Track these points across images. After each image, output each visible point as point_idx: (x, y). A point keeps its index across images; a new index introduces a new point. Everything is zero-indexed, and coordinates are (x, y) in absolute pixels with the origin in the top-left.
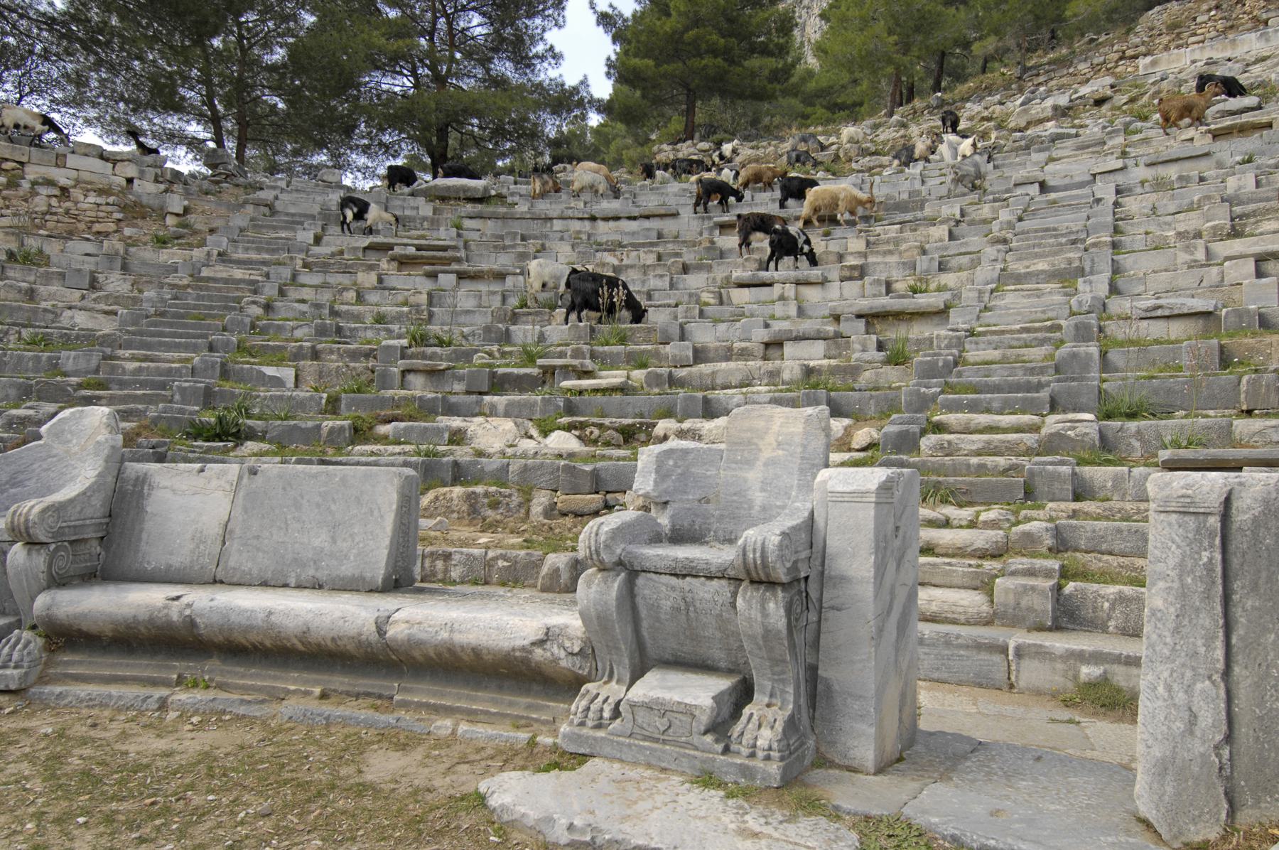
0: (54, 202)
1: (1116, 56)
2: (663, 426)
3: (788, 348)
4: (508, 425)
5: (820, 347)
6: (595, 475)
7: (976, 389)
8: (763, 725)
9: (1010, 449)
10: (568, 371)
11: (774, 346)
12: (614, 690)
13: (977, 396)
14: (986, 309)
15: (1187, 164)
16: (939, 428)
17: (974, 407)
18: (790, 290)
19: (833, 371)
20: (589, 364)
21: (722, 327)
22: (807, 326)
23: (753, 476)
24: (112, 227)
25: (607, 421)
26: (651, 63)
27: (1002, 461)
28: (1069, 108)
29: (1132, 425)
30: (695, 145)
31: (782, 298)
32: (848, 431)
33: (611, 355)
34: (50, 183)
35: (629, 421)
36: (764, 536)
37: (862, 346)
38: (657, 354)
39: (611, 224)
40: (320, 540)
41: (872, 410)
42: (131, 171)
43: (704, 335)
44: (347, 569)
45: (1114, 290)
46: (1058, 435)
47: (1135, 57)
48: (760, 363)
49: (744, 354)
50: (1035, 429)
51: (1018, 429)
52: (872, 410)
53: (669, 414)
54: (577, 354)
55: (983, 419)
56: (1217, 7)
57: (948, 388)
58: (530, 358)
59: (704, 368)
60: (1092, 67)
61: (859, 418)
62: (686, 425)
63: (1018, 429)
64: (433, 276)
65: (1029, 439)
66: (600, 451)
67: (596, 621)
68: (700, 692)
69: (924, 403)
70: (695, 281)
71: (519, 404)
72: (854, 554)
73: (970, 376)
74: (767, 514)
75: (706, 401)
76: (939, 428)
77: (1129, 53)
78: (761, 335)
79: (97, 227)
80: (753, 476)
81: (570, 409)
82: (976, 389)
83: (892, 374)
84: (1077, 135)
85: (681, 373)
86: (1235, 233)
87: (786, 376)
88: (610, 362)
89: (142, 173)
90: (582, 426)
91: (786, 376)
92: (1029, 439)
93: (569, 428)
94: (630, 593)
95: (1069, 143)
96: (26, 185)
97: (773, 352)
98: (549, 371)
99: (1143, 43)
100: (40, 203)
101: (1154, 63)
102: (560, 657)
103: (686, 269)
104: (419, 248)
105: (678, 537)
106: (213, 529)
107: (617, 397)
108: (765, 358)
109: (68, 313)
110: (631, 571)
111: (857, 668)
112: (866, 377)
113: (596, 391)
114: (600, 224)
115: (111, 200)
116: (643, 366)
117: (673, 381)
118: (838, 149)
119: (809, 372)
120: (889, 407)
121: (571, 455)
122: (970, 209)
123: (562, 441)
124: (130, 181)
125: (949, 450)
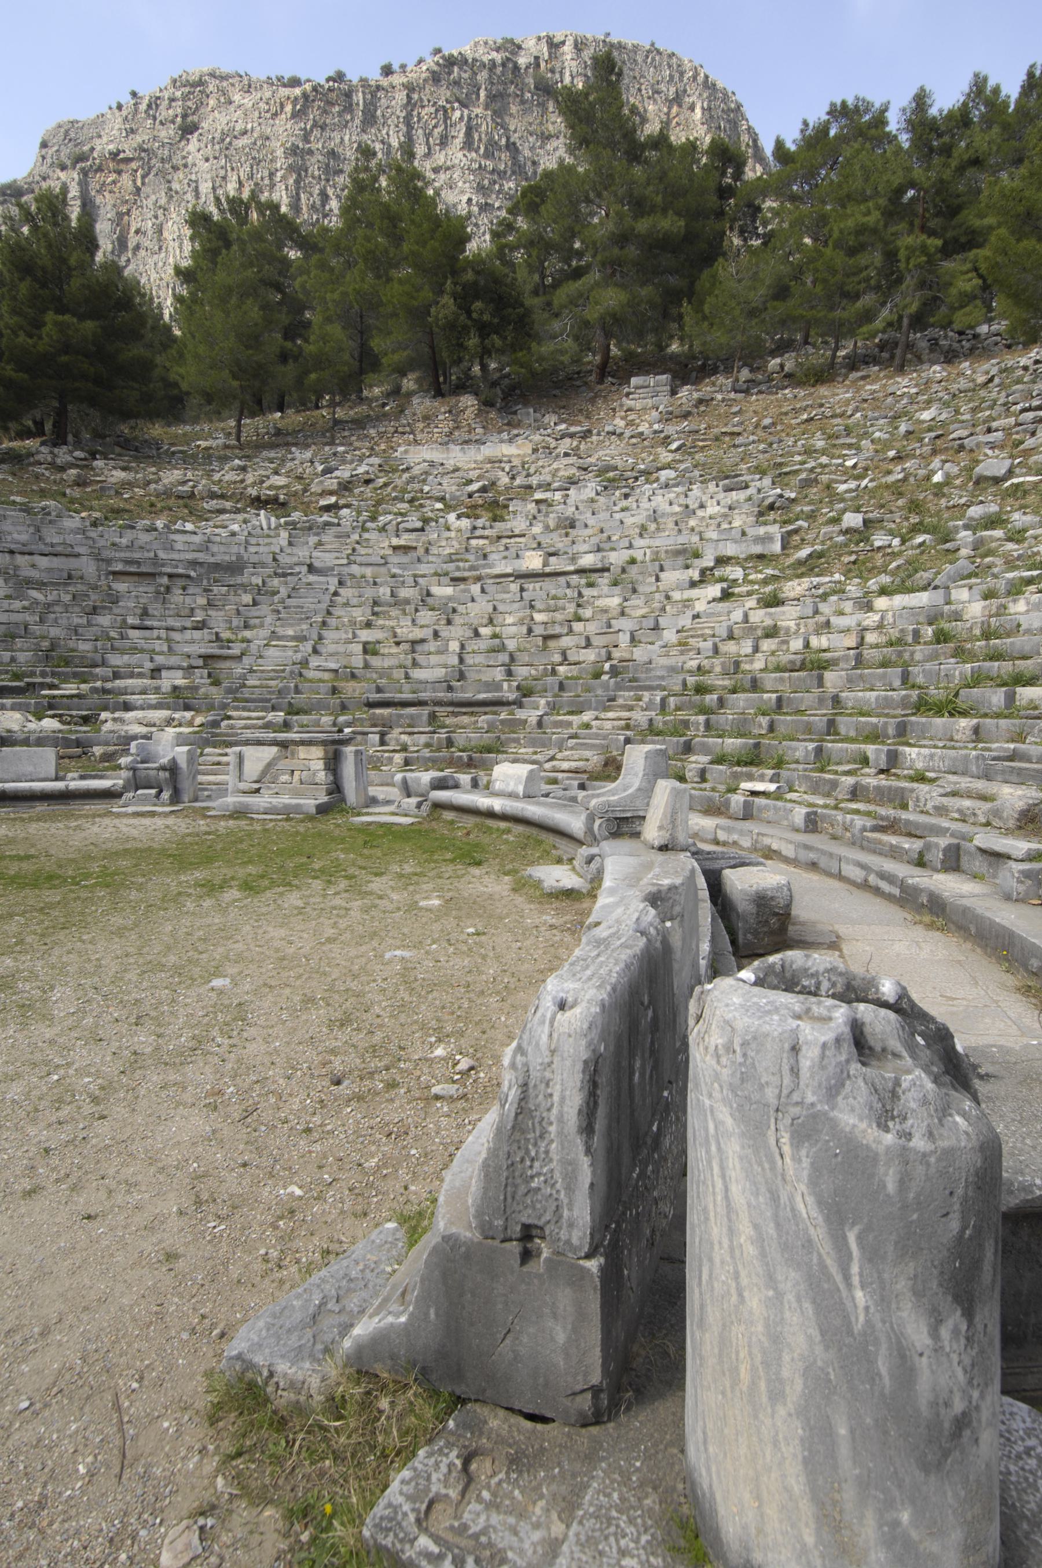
1: (392, 430)
2: (104, 715)
3: (164, 673)
4: (17, 715)
5: (180, 673)
6: (77, 739)
7: (247, 701)
8: (166, 795)
9: (254, 727)
10: (43, 686)
11: (156, 672)
12: (132, 794)
13: (246, 703)
14: (261, 657)
15: (376, 568)
16: (229, 718)
17: (244, 709)
18: (163, 633)
19: (187, 688)
20: (56, 681)
21: (126, 657)
22: (173, 660)
23: (160, 748)
25: (74, 713)
26: (26, 376)
28: (349, 482)
29: (295, 718)
30: (71, 452)
31: (159, 638)
32: (193, 718)
33: (63, 673)
35: (85, 713)
36: (164, 761)
37: (200, 677)
38: (91, 673)
39: (27, 557)
40: (30, 769)
41: (204, 708)
43: (116, 660)
44: (42, 776)
45: (315, 651)
46: (270, 722)
47: (404, 433)
48: (150, 681)
49: (140, 675)
50: (263, 718)
51: (258, 718)
52: (204, 708)
53: (105, 709)
54: (43, 674)
55: (246, 714)
56: (450, 412)
57: (236, 699)
58: (17, 677)
59: (119, 683)
60: (379, 433)
61: (198, 711)
62: (117, 715)
63: (258, 718)
65: (260, 722)
66: (73, 728)
67: (127, 781)
68: (153, 791)
69: (224, 706)
70: (104, 620)
71: (20, 704)
72: (183, 763)
73: (246, 693)
74: (164, 757)
75: (125, 703)
76: (229, 718)
77: (400, 429)
78: (149, 665)
80: (160, 748)
81: (51, 707)
82: (247, 701)
83: (213, 689)
84: (339, 525)
85: (109, 685)
86: (368, 625)
87: (164, 690)
88: (66, 679)
90: (61, 716)
91: (164, 690)
92: (260, 722)
93: (53, 716)
94: (134, 774)
95: (335, 529)
97: (156, 674)
98: (31, 686)
99: (409, 425)
101: (406, 452)
102: (118, 788)
103: (95, 611)
105: (142, 762)
107: (76, 700)
108: (153, 678)
110: (134, 770)
111: (185, 784)
112: (202, 690)
113: (63, 696)
114: (18, 556)
116: (85, 682)
117: (105, 691)
118: (194, 487)
119: (175, 688)
120: (211, 707)
121: (60, 731)
122: (268, 580)
123: (50, 724)
125: (232, 727)
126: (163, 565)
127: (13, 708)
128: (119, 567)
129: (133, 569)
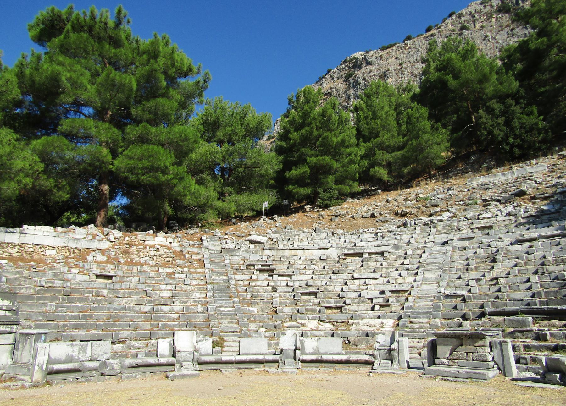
0: (155, 252)
24: (171, 259)
27: (422, 330)
34: (153, 246)
42: (171, 240)
44: (336, 352)
57: (413, 313)
64: (272, 276)
79: (167, 259)
89: (174, 240)
96: (148, 247)
100: (152, 253)
104: (262, 265)
106: (315, 347)
109: (195, 293)
115: (171, 251)
124: (171, 243)
126: (365, 249)
127: (314, 319)
128: (346, 251)
129: (352, 251)
